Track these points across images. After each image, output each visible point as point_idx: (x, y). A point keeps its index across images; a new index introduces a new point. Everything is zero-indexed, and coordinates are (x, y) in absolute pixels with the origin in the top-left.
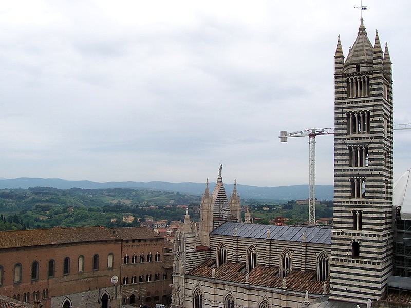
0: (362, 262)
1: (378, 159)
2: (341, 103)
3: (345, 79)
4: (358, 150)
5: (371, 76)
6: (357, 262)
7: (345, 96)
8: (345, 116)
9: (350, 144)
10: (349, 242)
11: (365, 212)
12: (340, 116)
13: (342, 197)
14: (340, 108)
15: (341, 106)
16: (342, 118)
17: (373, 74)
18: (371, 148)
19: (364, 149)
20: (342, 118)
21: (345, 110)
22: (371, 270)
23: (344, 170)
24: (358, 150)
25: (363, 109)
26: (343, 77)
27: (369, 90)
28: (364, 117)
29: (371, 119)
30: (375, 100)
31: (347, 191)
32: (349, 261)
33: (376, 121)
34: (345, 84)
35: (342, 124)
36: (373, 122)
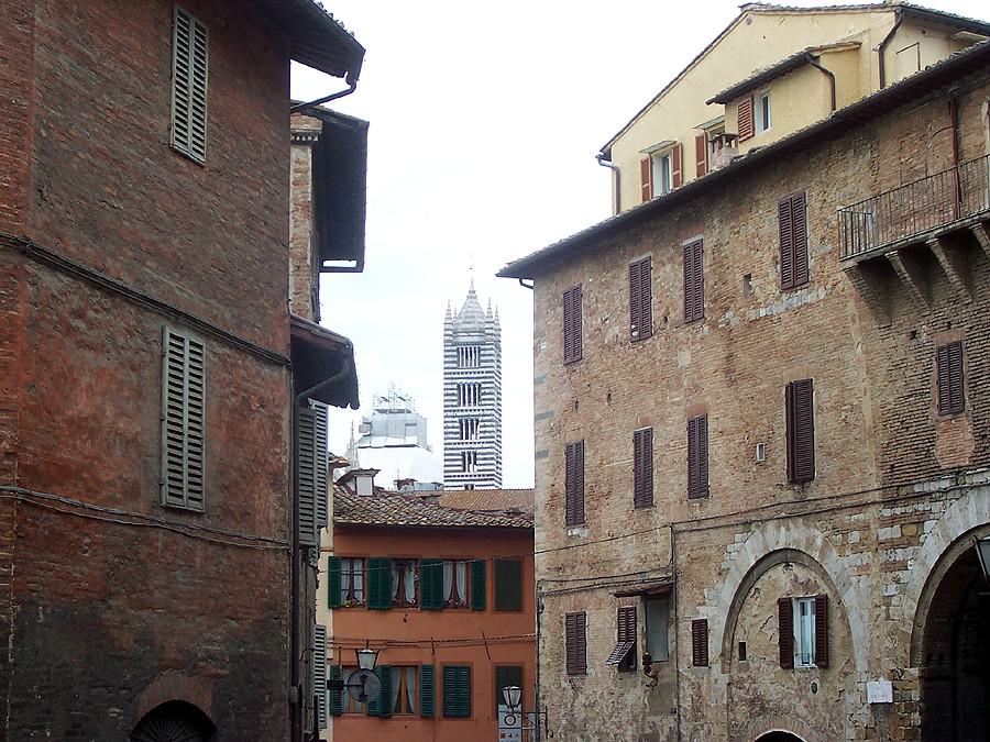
1: (490, 432)
3: (455, 348)
5: (482, 347)
7: (455, 365)
8: (455, 386)
12: (450, 387)
21: (454, 381)
25: (474, 381)
27: (480, 361)
28: (475, 389)
36: (485, 394)
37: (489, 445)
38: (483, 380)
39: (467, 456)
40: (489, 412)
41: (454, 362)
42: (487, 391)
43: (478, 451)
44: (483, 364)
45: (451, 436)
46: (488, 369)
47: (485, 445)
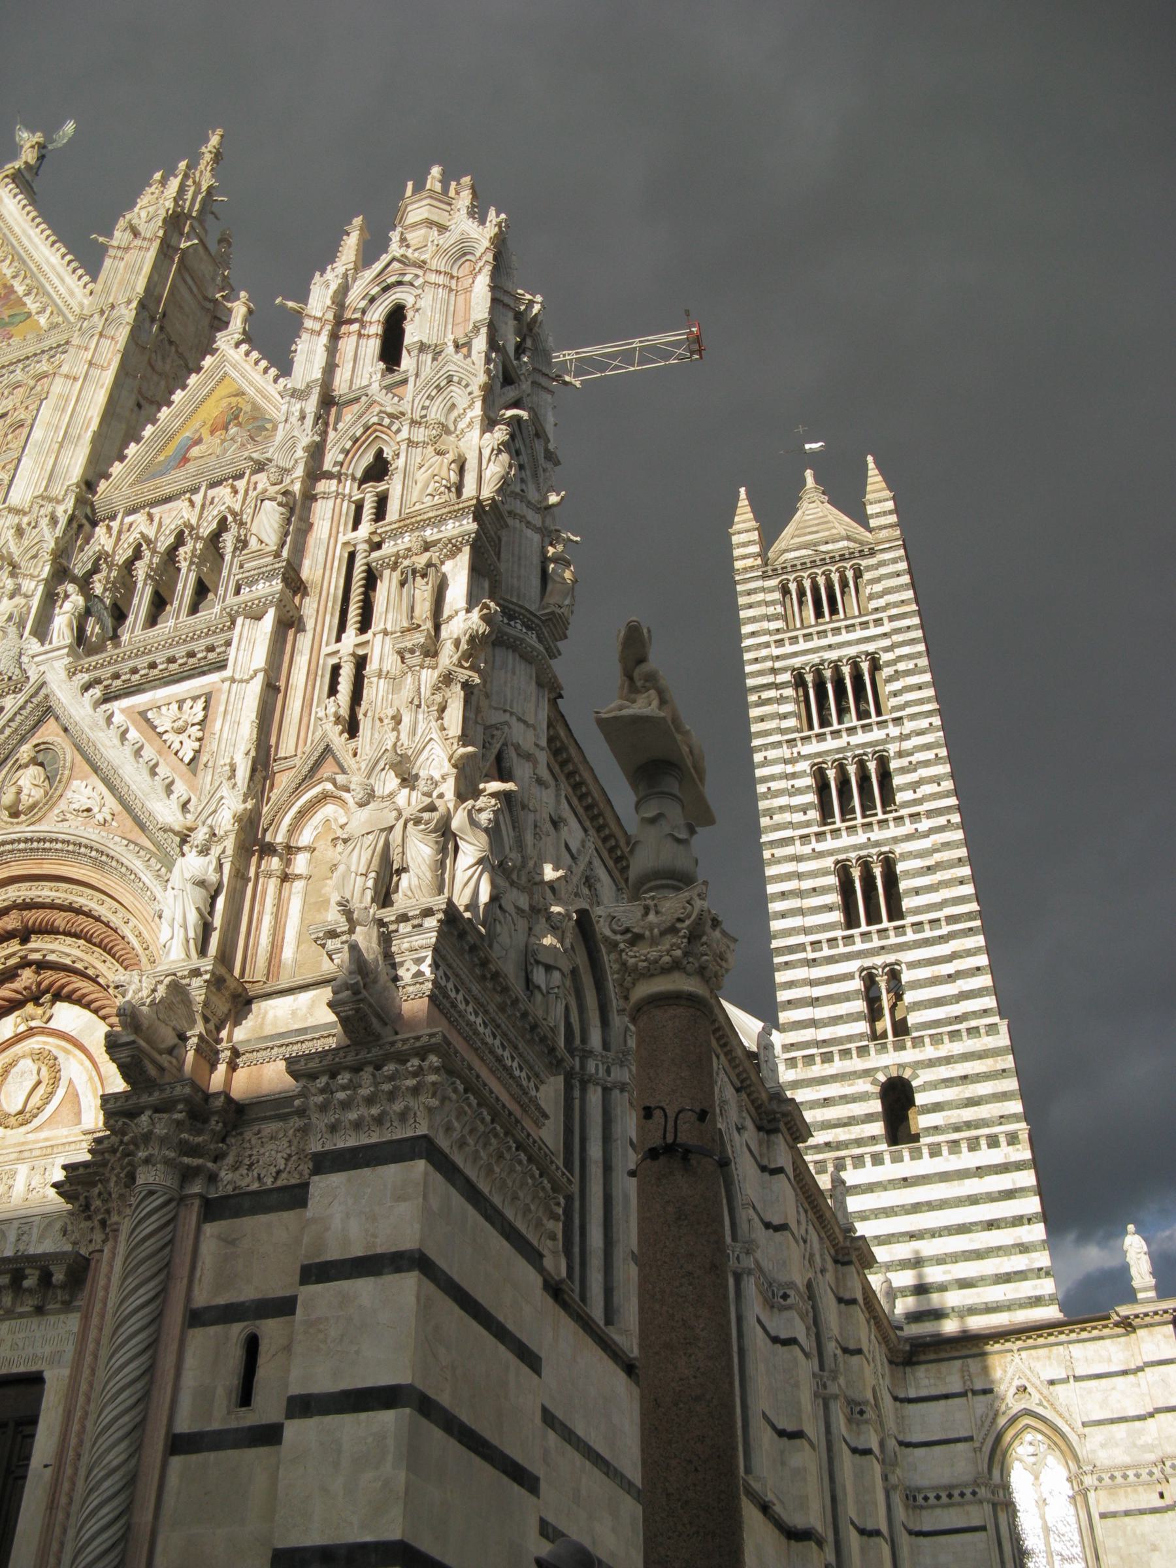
0: (935, 1151)
2: (767, 645)
3: (774, 582)
4: (852, 769)
5: (864, 563)
6: (916, 1155)
7: (780, 624)
8: (786, 677)
9: (819, 754)
10: (863, 1086)
11: (912, 965)
13: (806, 931)
14: (765, 659)
15: (764, 652)
16: (777, 686)
17: (872, 553)
18: (900, 754)
19: (872, 766)
20: (777, 686)
21: (778, 665)
22: (980, 1172)
23: (804, 838)
24: (852, 769)
25: (852, 651)
26: (765, 577)
28: (857, 678)
29: (887, 672)
30: (892, 618)
31: (830, 908)
32: (877, 1159)
33: (908, 673)
34: (777, 595)
35: (780, 700)
36: (897, 675)
37: (941, 821)
38: (886, 642)
39: (856, 873)
40: (924, 723)
41: (775, 617)
42: (901, 666)
43: (899, 849)
44: (873, 604)
45: (787, 817)
46: (894, 611)
47: (925, 825)
